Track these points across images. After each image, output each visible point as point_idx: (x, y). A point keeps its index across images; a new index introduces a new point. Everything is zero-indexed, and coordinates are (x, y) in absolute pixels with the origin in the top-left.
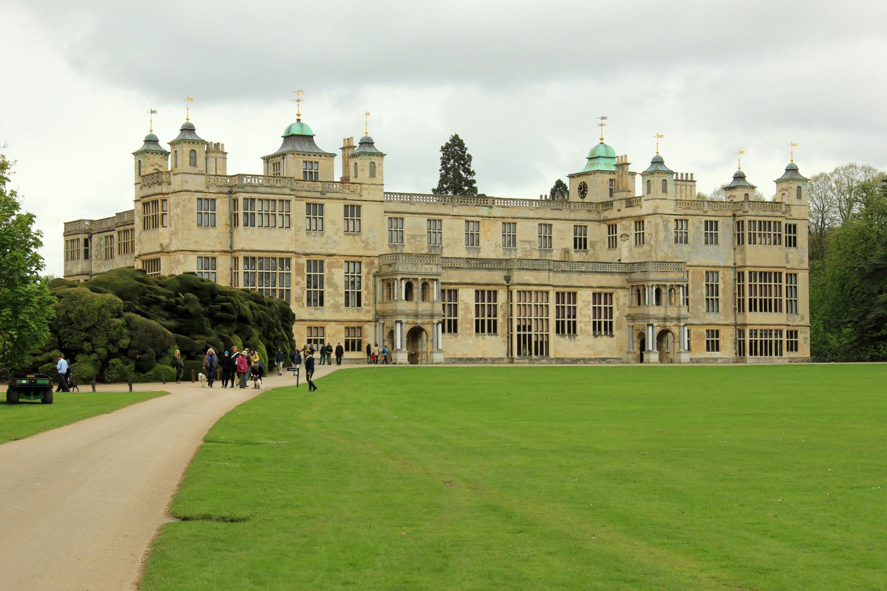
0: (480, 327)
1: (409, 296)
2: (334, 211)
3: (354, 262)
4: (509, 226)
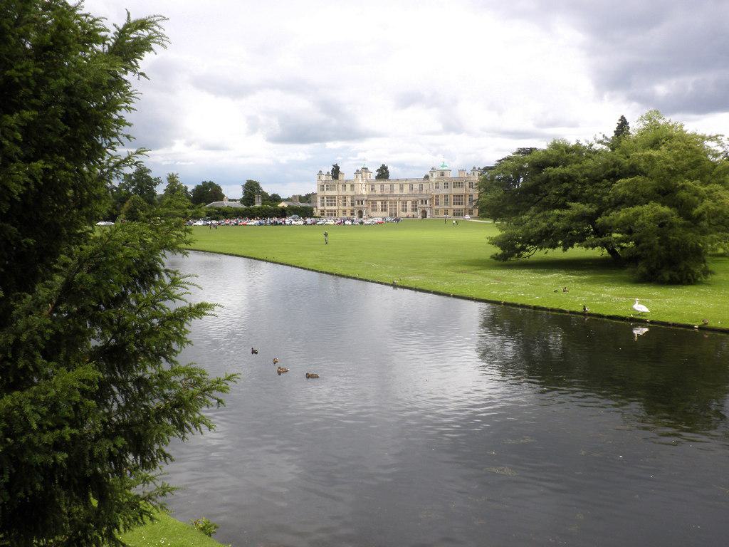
0: (382, 210)
1: (358, 204)
2: (348, 186)
3: (352, 197)
4: (411, 185)
